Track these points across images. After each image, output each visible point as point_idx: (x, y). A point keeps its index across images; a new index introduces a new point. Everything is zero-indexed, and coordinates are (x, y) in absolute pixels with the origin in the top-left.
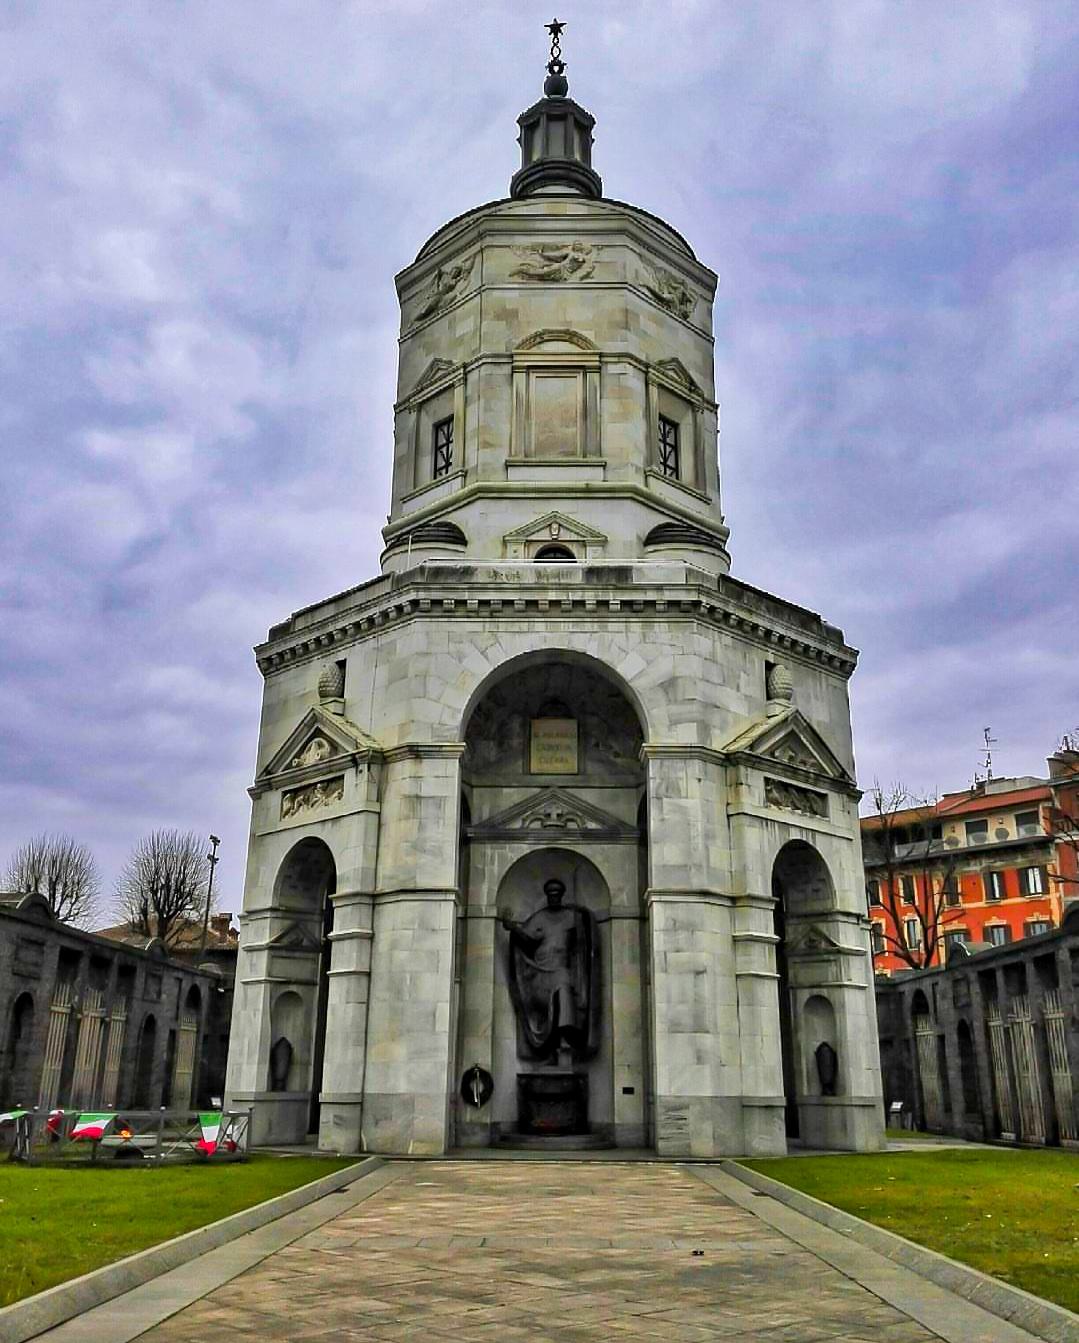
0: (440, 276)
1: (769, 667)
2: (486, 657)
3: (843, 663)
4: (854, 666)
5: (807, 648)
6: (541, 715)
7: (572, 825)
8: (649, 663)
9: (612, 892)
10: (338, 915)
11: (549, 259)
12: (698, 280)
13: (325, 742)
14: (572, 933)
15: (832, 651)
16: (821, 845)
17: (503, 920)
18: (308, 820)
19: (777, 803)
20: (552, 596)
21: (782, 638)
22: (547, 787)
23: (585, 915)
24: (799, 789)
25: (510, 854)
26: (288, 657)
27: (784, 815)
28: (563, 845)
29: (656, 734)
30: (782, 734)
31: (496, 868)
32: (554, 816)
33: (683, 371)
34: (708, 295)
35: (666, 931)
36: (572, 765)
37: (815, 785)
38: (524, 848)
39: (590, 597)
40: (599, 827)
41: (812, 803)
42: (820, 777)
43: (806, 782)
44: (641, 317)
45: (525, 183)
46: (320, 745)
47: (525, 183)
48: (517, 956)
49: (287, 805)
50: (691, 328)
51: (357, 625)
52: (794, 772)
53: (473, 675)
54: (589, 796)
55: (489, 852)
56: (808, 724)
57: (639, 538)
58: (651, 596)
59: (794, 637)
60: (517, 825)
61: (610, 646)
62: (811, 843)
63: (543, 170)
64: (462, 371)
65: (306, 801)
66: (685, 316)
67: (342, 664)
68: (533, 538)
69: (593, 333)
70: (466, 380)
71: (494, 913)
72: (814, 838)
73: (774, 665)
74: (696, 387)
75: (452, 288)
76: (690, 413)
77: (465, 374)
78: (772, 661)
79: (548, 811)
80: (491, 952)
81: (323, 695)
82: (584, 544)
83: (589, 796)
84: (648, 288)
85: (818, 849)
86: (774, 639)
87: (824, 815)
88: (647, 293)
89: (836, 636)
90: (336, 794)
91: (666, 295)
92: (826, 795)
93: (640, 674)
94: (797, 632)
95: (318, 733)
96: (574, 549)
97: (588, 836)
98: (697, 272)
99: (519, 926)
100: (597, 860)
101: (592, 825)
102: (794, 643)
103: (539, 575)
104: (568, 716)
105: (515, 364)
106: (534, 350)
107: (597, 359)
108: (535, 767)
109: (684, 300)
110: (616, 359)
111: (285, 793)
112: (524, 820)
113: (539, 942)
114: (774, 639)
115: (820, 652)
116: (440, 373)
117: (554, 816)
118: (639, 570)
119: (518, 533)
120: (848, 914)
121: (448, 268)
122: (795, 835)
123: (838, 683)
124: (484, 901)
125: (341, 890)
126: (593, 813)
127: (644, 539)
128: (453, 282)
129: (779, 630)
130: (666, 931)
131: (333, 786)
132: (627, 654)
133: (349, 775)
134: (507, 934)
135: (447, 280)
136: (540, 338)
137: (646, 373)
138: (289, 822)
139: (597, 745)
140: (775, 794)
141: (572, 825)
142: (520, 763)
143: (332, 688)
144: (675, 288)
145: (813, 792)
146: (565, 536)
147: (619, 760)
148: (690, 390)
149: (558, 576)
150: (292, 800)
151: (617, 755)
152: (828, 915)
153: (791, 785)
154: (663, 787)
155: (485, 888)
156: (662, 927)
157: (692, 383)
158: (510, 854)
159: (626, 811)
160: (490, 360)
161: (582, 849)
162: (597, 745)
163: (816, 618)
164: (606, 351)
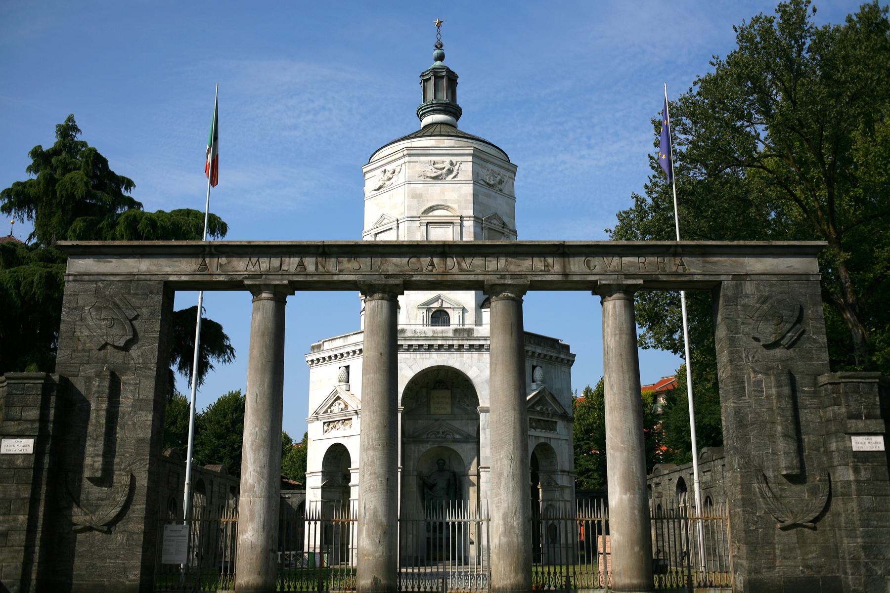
0: (385, 171)
1: (534, 367)
2: (412, 370)
3: (568, 361)
4: (573, 361)
5: (551, 357)
6: (434, 388)
7: (448, 436)
8: (481, 371)
9: (466, 465)
10: (352, 476)
11: (437, 169)
12: (508, 170)
13: (341, 402)
14: (449, 480)
15: (562, 356)
16: (553, 444)
17: (420, 476)
18: (337, 436)
19: (535, 428)
20: (440, 342)
21: (540, 354)
22: (438, 420)
23: (454, 474)
24: (544, 421)
25: (422, 449)
26: (321, 360)
27: (538, 433)
28: (444, 445)
29: (484, 402)
30: (538, 398)
31: (416, 455)
32: (441, 433)
33: (500, 219)
34: (512, 175)
35: (486, 482)
36: (449, 410)
37: (552, 418)
38: (428, 446)
39: (456, 343)
40: (460, 437)
41: (550, 426)
42: (555, 414)
43: (548, 417)
44: (480, 196)
45: (424, 111)
46: (339, 404)
47: (424, 111)
48: (425, 491)
49: (326, 428)
50: (505, 195)
51: (354, 352)
52: (542, 413)
53: (406, 377)
54: (457, 424)
55: (413, 448)
56: (550, 393)
57: (478, 304)
58: (482, 342)
59: (545, 353)
60: (425, 436)
61: (464, 365)
62: (549, 443)
63: (433, 107)
64: (396, 222)
65: (335, 427)
66: (501, 191)
67: (347, 367)
68: (431, 306)
69: (457, 205)
70: (398, 227)
71: (415, 473)
72: (550, 440)
73: (536, 366)
74: (507, 226)
75: (390, 179)
76: (503, 238)
77: (398, 224)
78: (535, 364)
79: (438, 430)
80: (415, 489)
81: (340, 381)
82: (454, 309)
83: (457, 424)
84: (485, 182)
85: (552, 445)
86: (536, 355)
87: (555, 430)
88: (484, 183)
89: (567, 347)
90: (349, 426)
91: (492, 183)
92: (556, 422)
93: (477, 376)
94: (547, 351)
95: (338, 398)
96: (448, 311)
97: (455, 441)
98: (507, 166)
99: (426, 478)
100: (459, 451)
101: (457, 436)
102: (545, 355)
103: (434, 332)
104: (447, 388)
105: (421, 221)
106: (430, 214)
107: (459, 218)
108: (432, 411)
109: (501, 182)
110: (468, 219)
111: (324, 423)
112: (428, 435)
113: (434, 485)
114: (536, 355)
115: (557, 358)
116: (385, 221)
117: (441, 433)
118: (477, 330)
119: (424, 304)
120: (563, 471)
121: (389, 168)
122: (542, 440)
123: (567, 370)
124: (411, 468)
125: (353, 466)
126: (458, 431)
127: (480, 305)
128: (391, 176)
129: (539, 351)
130: (486, 482)
131: (347, 422)
132: (472, 367)
133: (354, 417)
134: (421, 482)
135: (388, 174)
136: (432, 209)
137: (482, 224)
138: (327, 435)
139: (459, 401)
140: (534, 424)
141: (448, 436)
142: (426, 409)
143: (344, 378)
144: (496, 177)
145: (551, 421)
146: (445, 305)
147: (469, 408)
148: (503, 228)
149: (442, 332)
150: (328, 426)
151: (468, 405)
152: (554, 472)
153: (541, 420)
154: (486, 424)
155: (412, 463)
156: (485, 480)
157: (504, 224)
158: (422, 449)
159: (471, 430)
160: (410, 219)
161: (454, 447)
162: (459, 401)
163: (556, 341)
164: (464, 215)
